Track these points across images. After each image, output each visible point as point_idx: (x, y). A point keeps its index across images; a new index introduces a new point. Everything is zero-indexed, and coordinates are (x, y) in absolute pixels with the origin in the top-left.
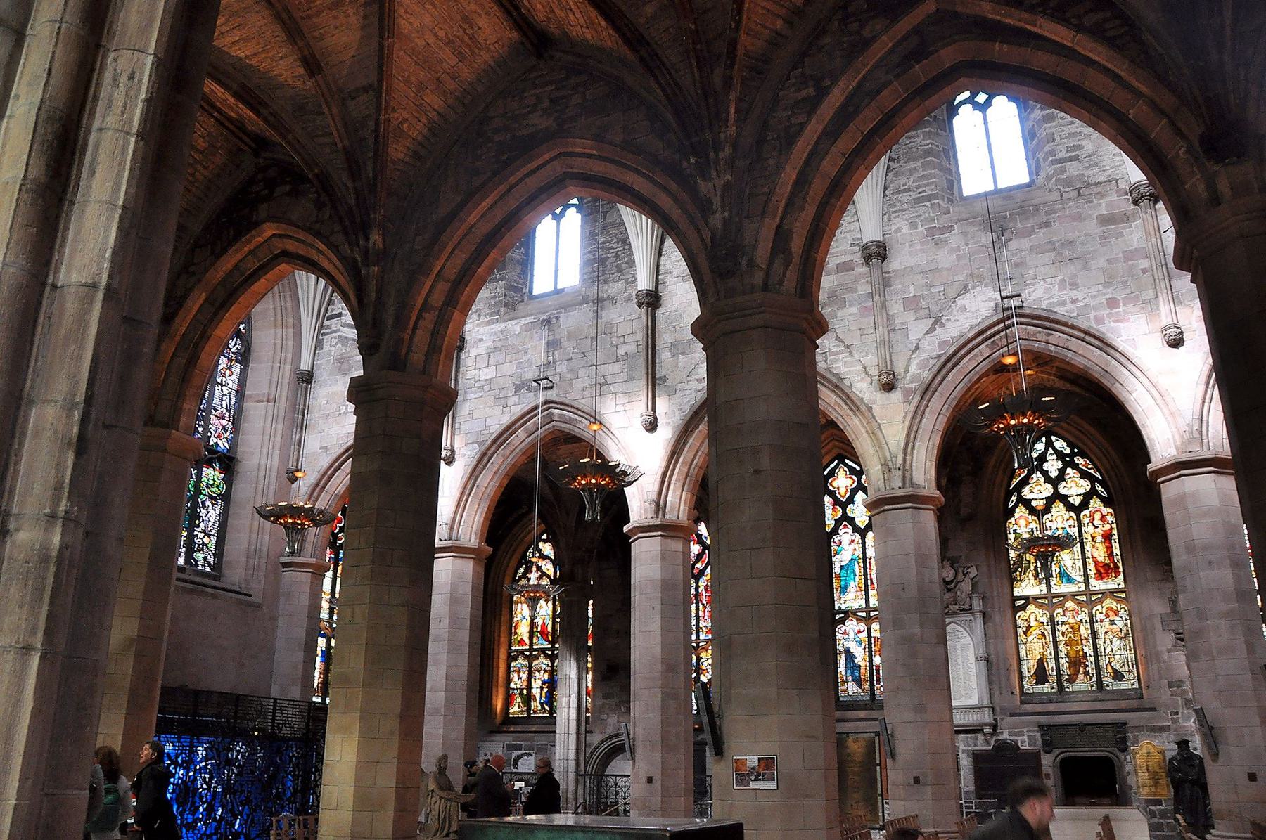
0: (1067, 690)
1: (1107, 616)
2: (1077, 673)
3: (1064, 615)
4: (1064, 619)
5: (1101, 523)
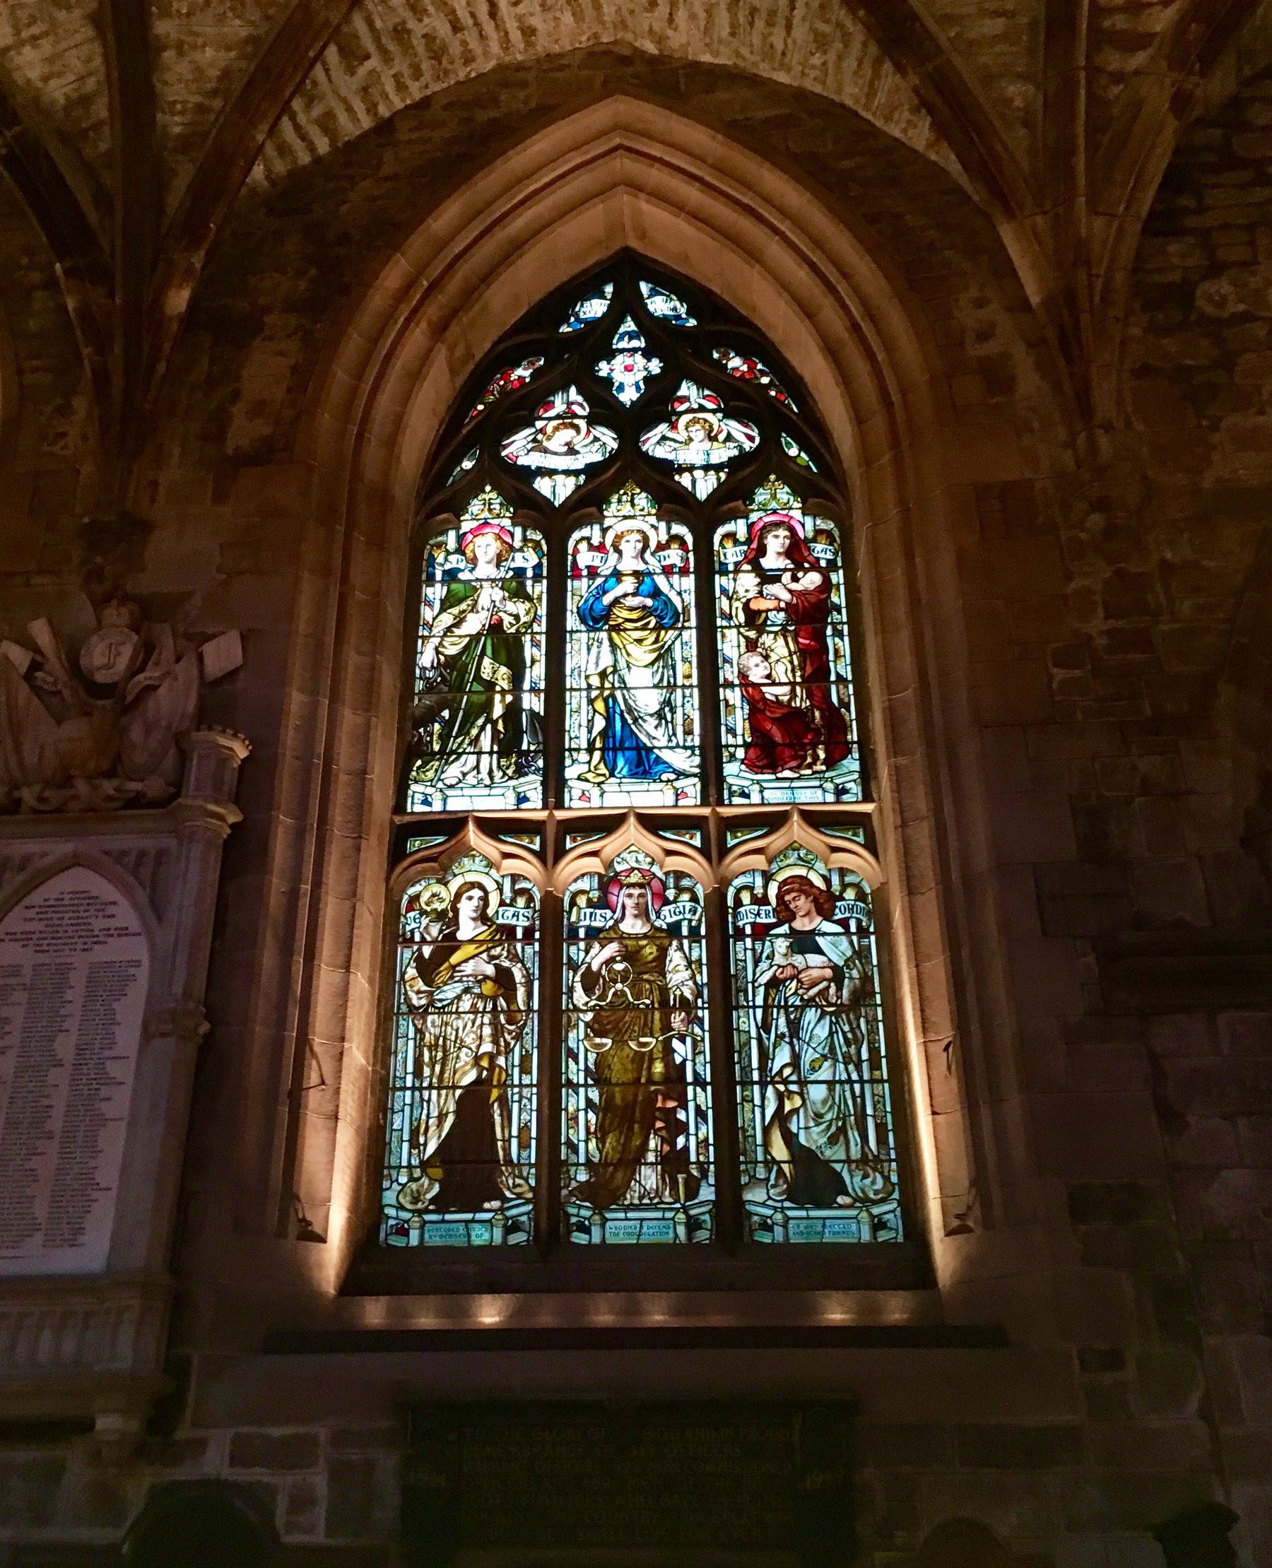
0: (579, 1238)
1: (785, 913)
2: (635, 1159)
3: (603, 903)
4: (601, 919)
5: (784, 563)
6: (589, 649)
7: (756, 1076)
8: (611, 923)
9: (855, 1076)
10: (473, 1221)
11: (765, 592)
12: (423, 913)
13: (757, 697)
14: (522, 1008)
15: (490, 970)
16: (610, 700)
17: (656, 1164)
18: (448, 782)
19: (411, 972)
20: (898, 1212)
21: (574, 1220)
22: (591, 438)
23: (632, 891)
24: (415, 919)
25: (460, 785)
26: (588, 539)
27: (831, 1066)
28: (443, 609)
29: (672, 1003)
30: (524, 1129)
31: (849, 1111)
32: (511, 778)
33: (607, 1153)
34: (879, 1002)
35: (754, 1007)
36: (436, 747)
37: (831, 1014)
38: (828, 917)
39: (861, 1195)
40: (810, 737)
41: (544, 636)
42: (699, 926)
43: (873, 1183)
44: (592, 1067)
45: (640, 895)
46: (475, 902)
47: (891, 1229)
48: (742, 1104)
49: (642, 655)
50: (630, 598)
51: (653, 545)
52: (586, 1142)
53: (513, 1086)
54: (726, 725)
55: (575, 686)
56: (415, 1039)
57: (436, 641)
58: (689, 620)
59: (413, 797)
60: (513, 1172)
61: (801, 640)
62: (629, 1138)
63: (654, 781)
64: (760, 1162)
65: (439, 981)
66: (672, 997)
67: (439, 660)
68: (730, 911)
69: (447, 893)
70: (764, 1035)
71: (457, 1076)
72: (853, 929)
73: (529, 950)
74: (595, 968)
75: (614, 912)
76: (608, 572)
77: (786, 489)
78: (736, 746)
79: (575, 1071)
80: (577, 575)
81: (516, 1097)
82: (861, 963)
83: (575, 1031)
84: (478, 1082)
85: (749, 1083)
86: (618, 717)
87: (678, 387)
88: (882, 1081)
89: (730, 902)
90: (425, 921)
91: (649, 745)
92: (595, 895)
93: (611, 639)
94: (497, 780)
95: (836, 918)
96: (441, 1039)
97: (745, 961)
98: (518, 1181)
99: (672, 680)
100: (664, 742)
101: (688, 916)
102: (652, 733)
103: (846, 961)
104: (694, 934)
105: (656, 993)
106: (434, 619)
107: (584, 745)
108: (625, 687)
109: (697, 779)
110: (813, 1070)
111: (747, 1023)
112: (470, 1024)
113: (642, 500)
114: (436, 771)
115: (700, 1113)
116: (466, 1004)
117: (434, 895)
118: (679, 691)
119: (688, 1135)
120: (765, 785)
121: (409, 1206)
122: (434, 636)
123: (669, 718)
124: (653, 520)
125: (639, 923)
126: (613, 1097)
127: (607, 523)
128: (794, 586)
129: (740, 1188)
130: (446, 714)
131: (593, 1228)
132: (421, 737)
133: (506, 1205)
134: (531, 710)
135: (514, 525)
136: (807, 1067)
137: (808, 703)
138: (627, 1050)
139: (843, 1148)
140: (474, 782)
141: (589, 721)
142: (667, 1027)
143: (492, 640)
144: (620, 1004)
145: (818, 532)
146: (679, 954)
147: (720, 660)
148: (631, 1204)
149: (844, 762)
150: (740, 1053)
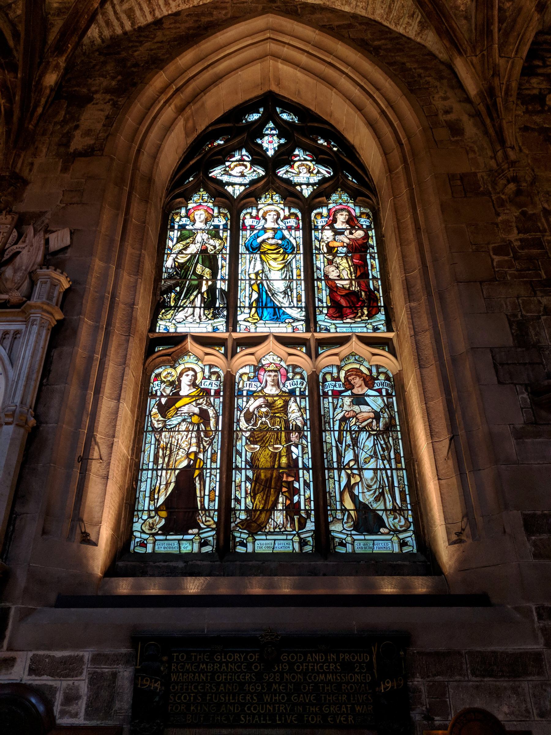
0: (240, 549)
1: (349, 385)
3: (256, 377)
6: (250, 262)
7: (335, 465)
8: (260, 388)
9: (387, 466)
10: (182, 540)
11: (336, 239)
12: (162, 382)
13: (333, 285)
14: (213, 429)
15: (197, 410)
16: (261, 285)
17: (283, 510)
18: (178, 320)
19: (155, 411)
20: (413, 536)
21: (238, 540)
22: (252, 170)
23: (271, 373)
24: (158, 385)
25: (184, 322)
26: (251, 213)
27: (375, 461)
28: (178, 242)
29: (291, 428)
30: (212, 490)
31: (385, 484)
32: (210, 320)
33: (256, 505)
34: (399, 429)
35: (334, 431)
36: (172, 304)
37: (374, 435)
38: (371, 388)
39: (393, 528)
40: (359, 304)
41: (228, 256)
42: (305, 390)
43: (399, 521)
44: (249, 460)
45: (275, 376)
46: (190, 377)
47: (410, 546)
48: (328, 479)
49: (276, 265)
50: (270, 240)
51: (282, 217)
52: (245, 498)
53: (206, 469)
54: (318, 298)
55: (243, 278)
56: (155, 444)
57: (174, 256)
58: (299, 250)
59: (159, 327)
60: (205, 514)
61: (354, 260)
62: (268, 497)
63: (282, 323)
64: (339, 510)
65: (169, 415)
66: (291, 425)
67: (175, 264)
68: (321, 384)
69: (174, 374)
70: (339, 445)
71: (177, 463)
72: (384, 394)
73: (217, 400)
74: (251, 410)
75: (261, 383)
76: (261, 228)
77: (346, 194)
78: (323, 307)
79: (240, 461)
80: (245, 228)
81: (208, 475)
82: (388, 410)
83: (240, 441)
84: (188, 466)
85: (331, 469)
86: (264, 293)
87: (294, 151)
88: (402, 469)
89: (321, 380)
90: (163, 386)
91: (279, 305)
92: (251, 375)
93: (261, 258)
94: (203, 320)
95: (375, 388)
96: (169, 445)
97: (329, 408)
98: (208, 519)
99: (291, 277)
100: (287, 305)
101: (299, 386)
102: (281, 300)
103: (381, 410)
104: (302, 396)
105: (283, 423)
106: (173, 246)
107: (247, 305)
108: (267, 279)
109: (303, 322)
110: (365, 463)
111: (330, 438)
112: (185, 437)
113: (277, 198)
114: (172, 315)
115: (306, 484)
116: (183, 427)
117: (168, 374)
118: (295, 282)
119: (300, 495)
120: (338, 325)
121: (147, 531)
122: (174, 253)
123: (290, 294)
124: (282, 206)
125: (274, 389)
126: (260, 474)
127: (260, 206)
128: (351, 236)
129: (327, 524)
130: (178, 289)
131: (248, 544)
132: (165, 299)
133: (201, 531)
134: (221, 288)
135: (214, 206)
136: (362, 461)
137: (359, 289)
138: (267, 451)
139: (383, 503)
140: (192, 321)
141: (250, 294)
142: (288, 440)
143: (202, 256)
144: (264, 429)
145: (362, 213)
146: (294, 404)
147: (315, 269)
148: (269, 531)
149: (377, 316)
150: (327, 453)
